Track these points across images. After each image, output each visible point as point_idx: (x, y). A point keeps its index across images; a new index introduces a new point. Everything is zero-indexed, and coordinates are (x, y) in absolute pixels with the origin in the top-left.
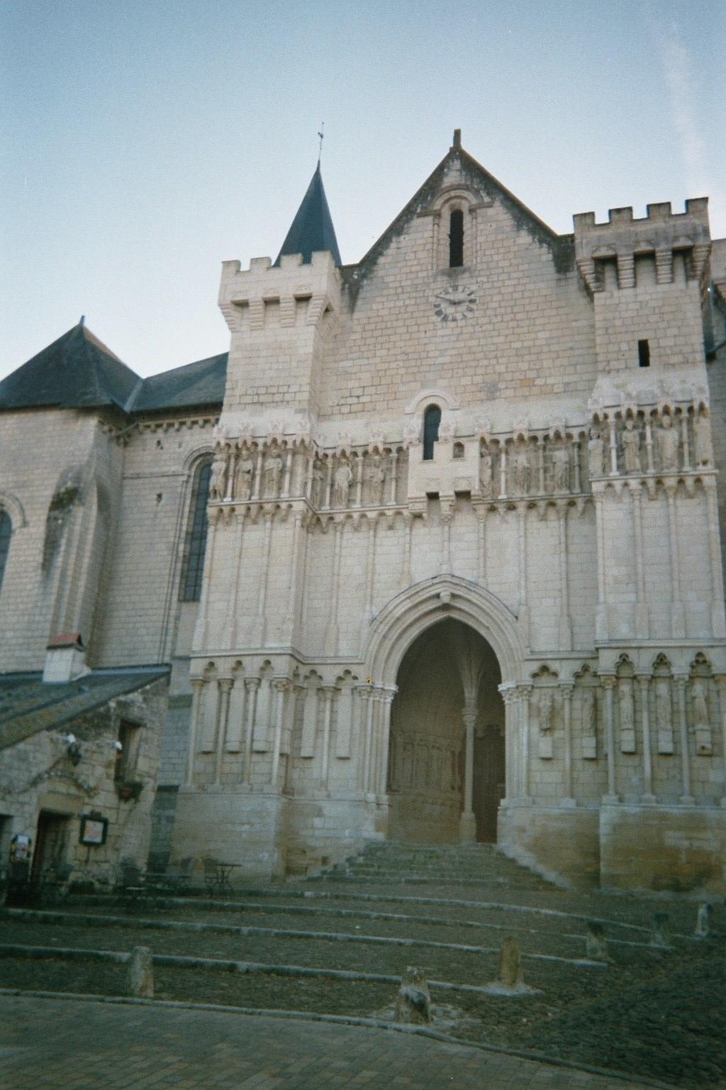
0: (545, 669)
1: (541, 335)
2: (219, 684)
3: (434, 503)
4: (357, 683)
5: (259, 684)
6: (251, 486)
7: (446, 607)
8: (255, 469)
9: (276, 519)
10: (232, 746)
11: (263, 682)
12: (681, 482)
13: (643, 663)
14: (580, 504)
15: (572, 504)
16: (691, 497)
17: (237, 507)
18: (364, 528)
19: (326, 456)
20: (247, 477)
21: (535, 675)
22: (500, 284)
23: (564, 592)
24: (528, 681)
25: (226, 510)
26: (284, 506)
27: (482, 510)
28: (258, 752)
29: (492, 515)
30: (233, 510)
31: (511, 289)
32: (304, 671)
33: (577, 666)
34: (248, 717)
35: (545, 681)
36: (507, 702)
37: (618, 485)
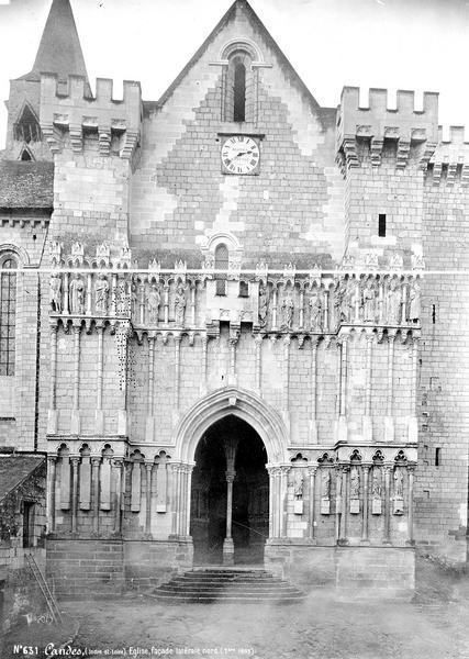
0: (299, 456)
1: (305, 196)
2: (70, 462)
3: (225, 330)
4: (170, 461)
5: (101, 462)
6: (84, 303)
7: (232, 407)
8: (86, 287)
9: (108, 331)
10: (85, 505)
11: (105, 460)
12: (399, 332)
13: (367, 457)
14: (327, 338)
15: (321, 338)
16: (404, 343)
17: (74, 320)
18: (171, 343)
19: (139, 280)
20: (80, 294)
21: (293, 460)
22: (275, 144)
23: (314, 403)
24: (288, 463)
25: (65, 321)
26: (112, 322)
27: (259, 337)
28: (105, 511)
29: (266, 340)
30: (70, 322)
31: (284, 151)
32: (131, 451)
33: (321, 455)
34: (96, 489)
35: (300, 463)
36: (271, 475)
37: (359, 330)
